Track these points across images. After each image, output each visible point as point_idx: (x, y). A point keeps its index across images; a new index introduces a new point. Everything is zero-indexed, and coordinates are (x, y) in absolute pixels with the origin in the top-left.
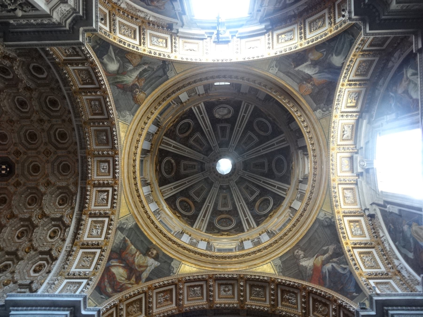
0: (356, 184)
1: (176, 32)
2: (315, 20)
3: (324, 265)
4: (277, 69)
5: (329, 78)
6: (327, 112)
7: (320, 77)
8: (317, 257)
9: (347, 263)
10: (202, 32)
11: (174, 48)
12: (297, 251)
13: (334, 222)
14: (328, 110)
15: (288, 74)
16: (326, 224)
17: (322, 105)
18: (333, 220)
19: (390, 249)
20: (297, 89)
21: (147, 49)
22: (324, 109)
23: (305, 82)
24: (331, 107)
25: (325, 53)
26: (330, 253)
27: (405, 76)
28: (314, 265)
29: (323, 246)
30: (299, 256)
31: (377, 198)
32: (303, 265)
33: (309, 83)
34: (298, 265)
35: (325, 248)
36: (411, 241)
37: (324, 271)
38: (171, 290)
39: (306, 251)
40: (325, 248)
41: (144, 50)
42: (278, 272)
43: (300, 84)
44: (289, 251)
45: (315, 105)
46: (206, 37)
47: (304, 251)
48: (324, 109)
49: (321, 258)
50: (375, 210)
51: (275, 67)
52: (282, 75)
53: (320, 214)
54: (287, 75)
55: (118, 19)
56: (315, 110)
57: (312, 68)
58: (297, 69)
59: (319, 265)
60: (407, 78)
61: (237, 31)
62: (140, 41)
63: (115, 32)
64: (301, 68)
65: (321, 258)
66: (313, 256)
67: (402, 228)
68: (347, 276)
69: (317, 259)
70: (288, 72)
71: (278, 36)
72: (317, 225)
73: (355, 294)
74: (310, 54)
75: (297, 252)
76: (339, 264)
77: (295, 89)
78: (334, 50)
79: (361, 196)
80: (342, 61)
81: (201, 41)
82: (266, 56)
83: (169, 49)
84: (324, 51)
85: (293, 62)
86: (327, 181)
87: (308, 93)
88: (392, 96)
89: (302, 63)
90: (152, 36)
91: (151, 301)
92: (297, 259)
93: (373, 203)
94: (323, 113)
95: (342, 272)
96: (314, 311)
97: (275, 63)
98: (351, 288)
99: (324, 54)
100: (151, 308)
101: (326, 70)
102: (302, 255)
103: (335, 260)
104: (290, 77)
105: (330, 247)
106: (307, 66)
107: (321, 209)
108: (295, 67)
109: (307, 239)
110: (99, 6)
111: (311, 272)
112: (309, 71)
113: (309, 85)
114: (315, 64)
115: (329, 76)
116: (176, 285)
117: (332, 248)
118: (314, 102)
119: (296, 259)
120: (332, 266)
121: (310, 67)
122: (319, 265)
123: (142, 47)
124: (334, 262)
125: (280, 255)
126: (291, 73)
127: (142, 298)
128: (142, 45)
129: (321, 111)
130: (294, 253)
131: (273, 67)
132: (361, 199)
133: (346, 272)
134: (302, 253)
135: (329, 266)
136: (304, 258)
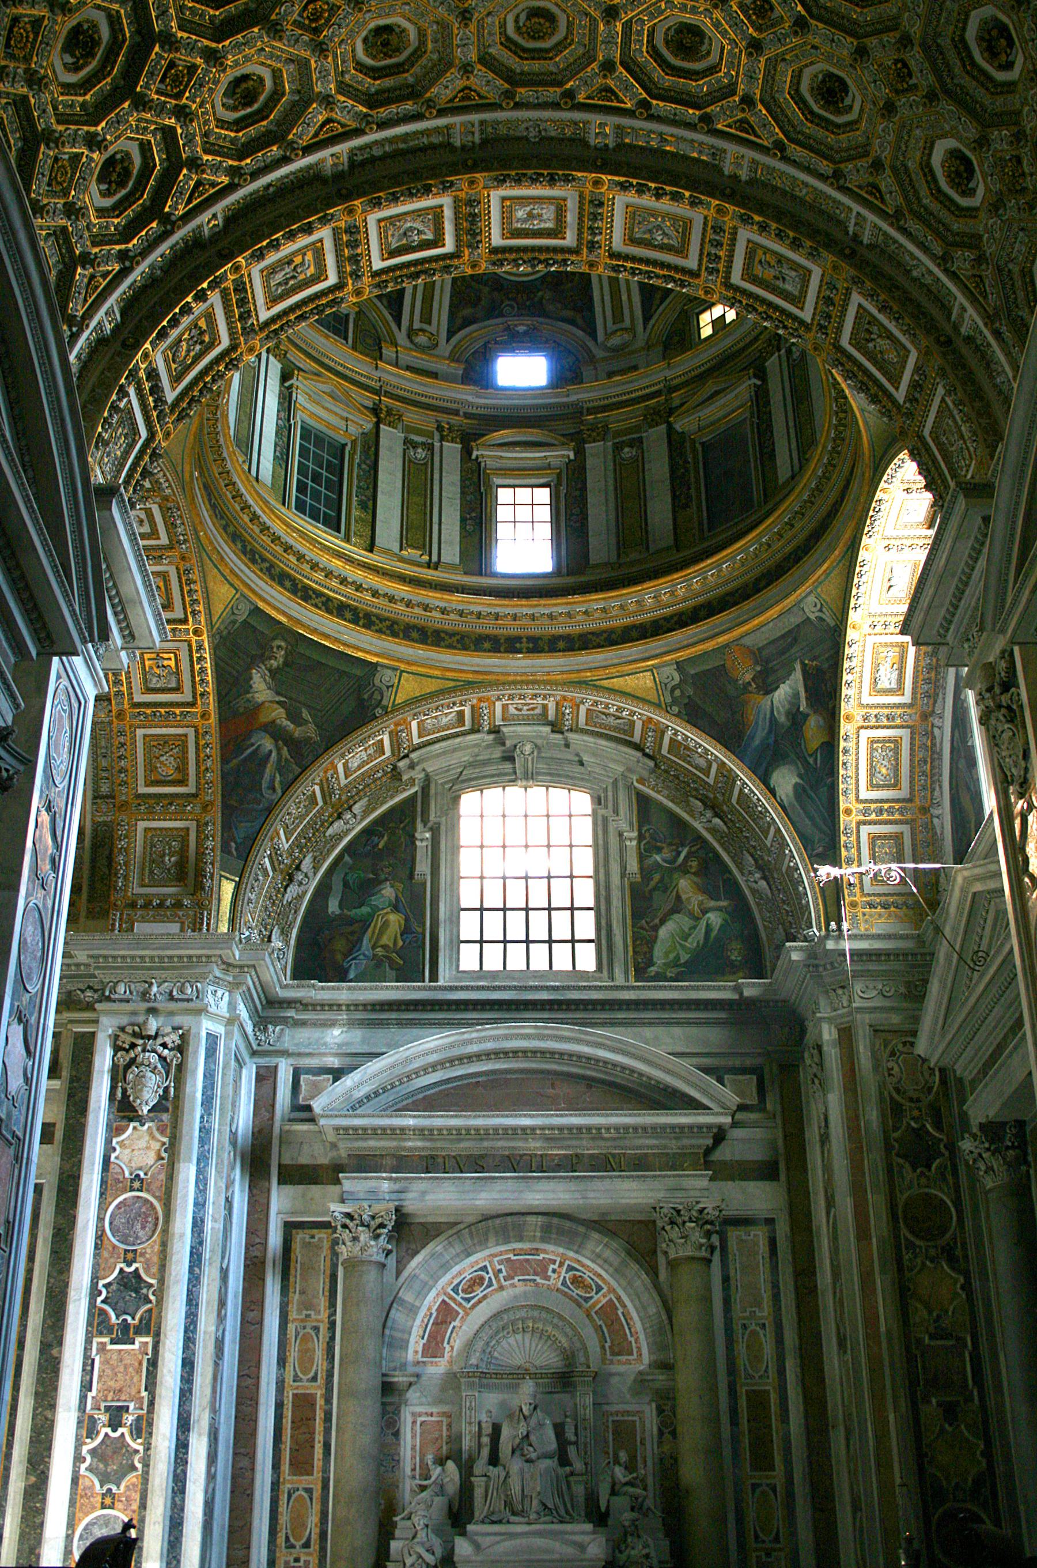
0: (474, 731)
2: (897, 751)
3: (266, 731)
4: (812, 617)
5: (752, 738)
6: (669, 700)
7: (761, 716)
8: (278, 703)
9: (287, 787)
12: (283, 644)
13: (375, 718)
14: (675, 701)
15: (792, 636)
16: (366, 697)
17: (690, 691)
18: (379, 711)
19: (332, 837)
20: (747, 641)
22: (677, 693)
23: (758, 668)
24: (678, 715)
25: (811, 760)
26: (297, 732)
27: (713, 904)
28: (259, 706)
29: (309, 708)
30: (270, 658)
31: (443, 784)
32: (251, 678)
33: (753, 679)
34: (249, 668)
35: (305, 714)
36: (365, 910)
37: (253, 740)
39: (287, 669)
40: (305, 714)
42: (219, 632)
43: (757, 655)
44: (280, 623)
45: (693, 672)
47: (286, 664)
48: (677, 693)
49: (278, 714)
50: (412, 781)
51: (819, 614)
52: (795, 620)
53: (389, 672)
54: (790, 632)
56: (679, 666)
57: (787, 707)
58: (798, 666)
59: (264, 718)
60: (704, 912)
64: (798, 675)
65: (278, 714)
66: (278, 694)
67: (386, 880)
68: (259, 802)
69: (276, 706)
70: (795, 640)
72: (358, 672)
73: (233, 844)
74: (822, 722)
75: (279, 647)
76: (280, 768)
77: (747, 634)
78: (807, 788)
79: (443, 744)
80: (780, 792)
82: (853, 616)
84: (816, 760)
85: (818, 669)
86: (480, 678)
87: (728, 664)
88: (679, 854)
89: (806, 691)
92: (263, 655)
93: (428, 779)
94: (669, 686)
95: (264, 785)
97: (828, 620)
98: (242, 831)
99: (811, 756)
101: (771, 740)
102: (274, 663)
103: (285, 751)
104: (783, 637)
105: (312, 726)
106: (796, 695)
107: (402, 672)
108: (803, 665)
109: (316, 656)
111: (241, 710)
112: (782, 693)
113: (748, 677)
114: (796, 719)
115: (757, 742)
117: (310, 731)
118: (704, 672)
119: (262, 655)
120: (271, 752)
121: (790, 703)
122: (264, 718)
124: (279, 753)
125: (261, 605)
126: (791, 645)
129: (673, 683)
130: (274, 639)
131: (821, 610)
132: (437, 746)
133: (267, 793)
134: (281, 660)
135: (267, 744)
136: (270, 671)
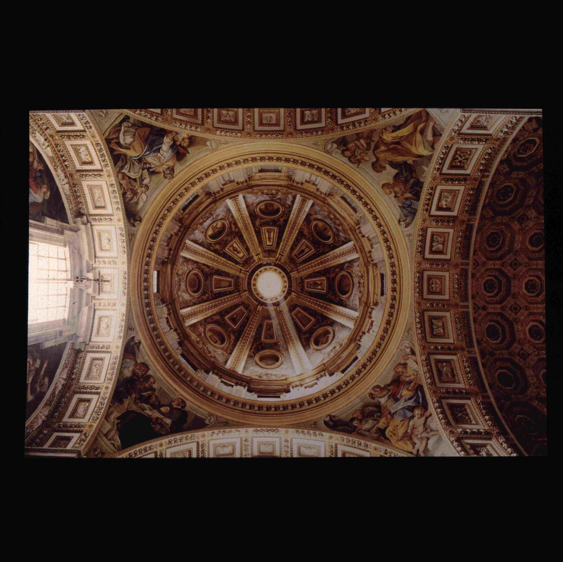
1: (84, 346)
10: (85, 309)
11: (104, 350)
21: (105, 385)
38: (438, 361)
41: (107, 388)
46: (93, 304)
55: (66, 419)
61: (87, 261)
62: (95, 393)
63: (82, 426)
71: (97, 207)
81: (97, 313)
83: (107, 356)
90: (88, 376)
91: (451, 391)
96: (462, 168)
100: (460, 389)
110: (46, 447)
116: (429, 354)
123: (102, 391)
127: (447, 404)
128: (99, 390)
